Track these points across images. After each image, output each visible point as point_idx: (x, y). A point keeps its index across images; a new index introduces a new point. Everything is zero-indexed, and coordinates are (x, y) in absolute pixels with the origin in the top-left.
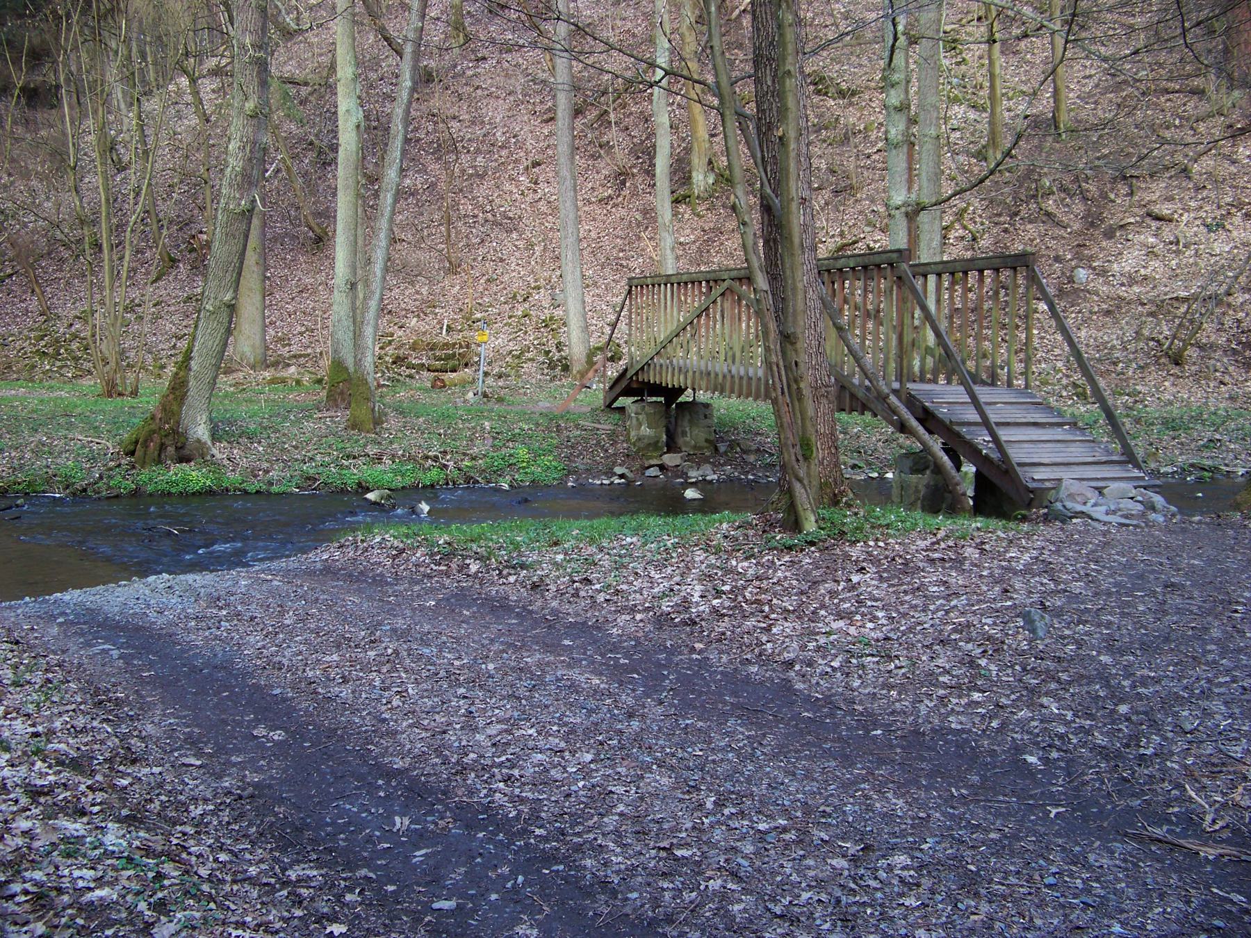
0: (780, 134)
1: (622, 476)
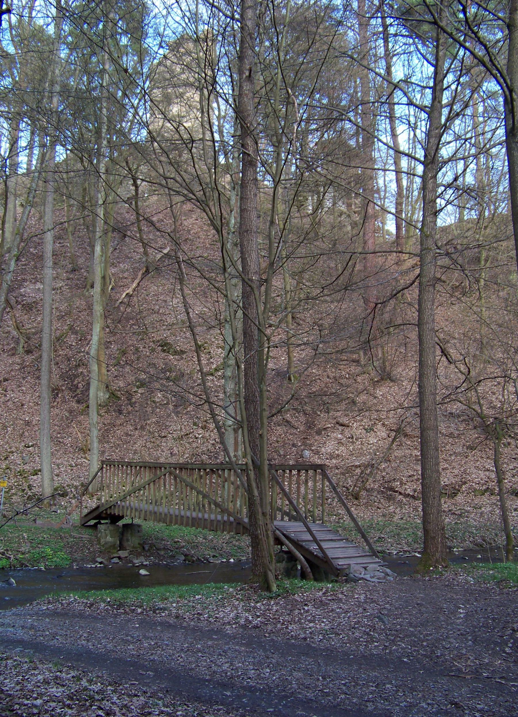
0: (260, 433)
1: (101, 563)
